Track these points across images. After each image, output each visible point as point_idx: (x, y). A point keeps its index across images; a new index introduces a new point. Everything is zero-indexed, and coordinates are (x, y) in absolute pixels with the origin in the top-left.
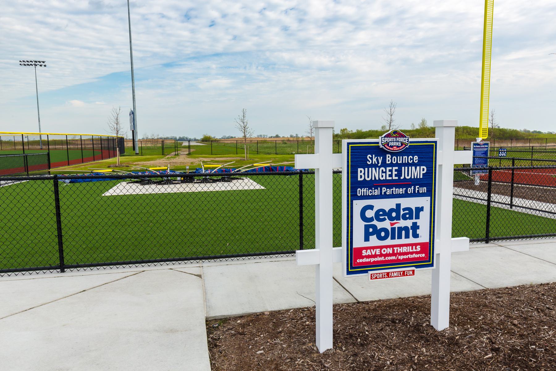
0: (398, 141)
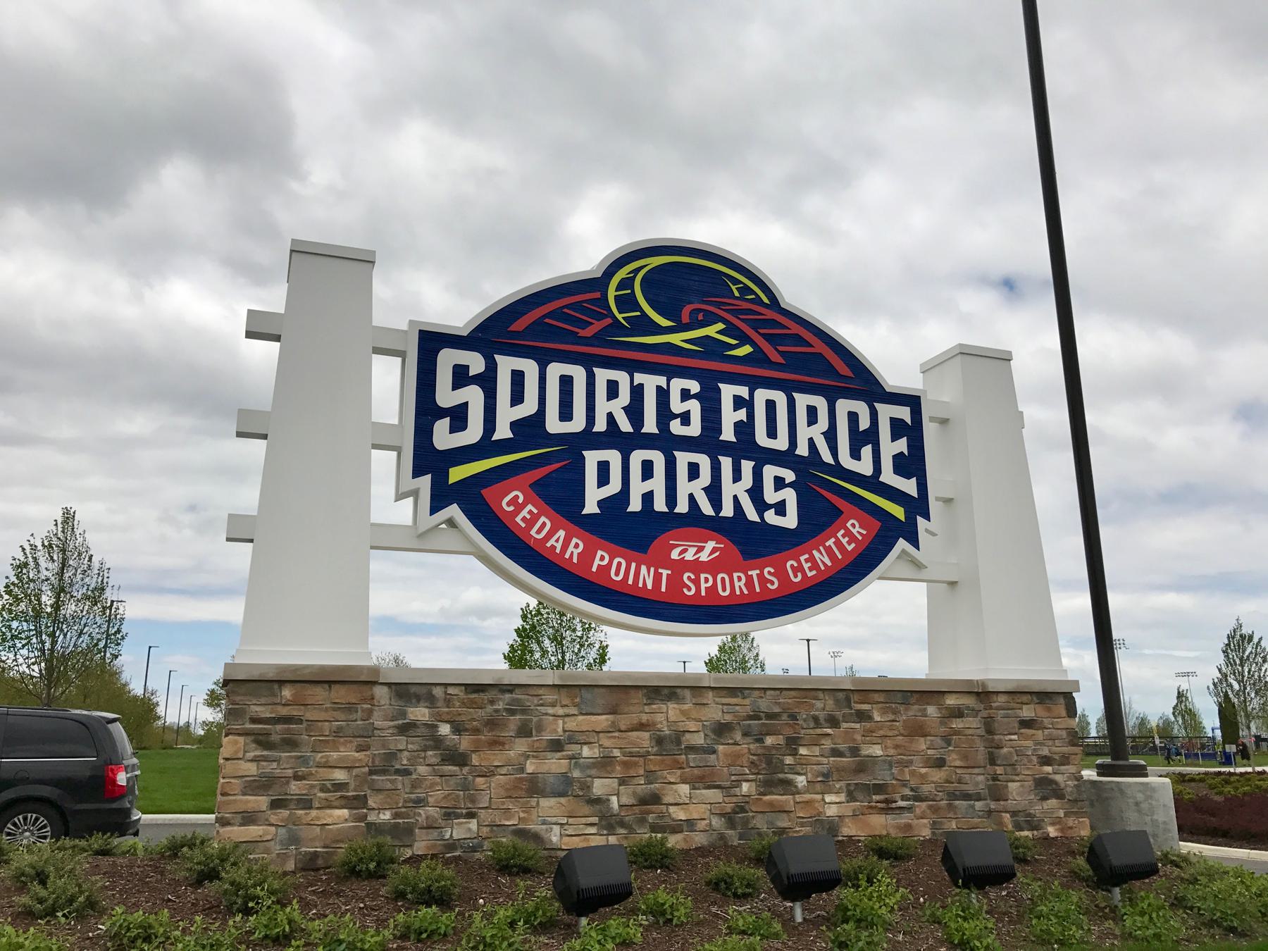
0: (745, 446)
